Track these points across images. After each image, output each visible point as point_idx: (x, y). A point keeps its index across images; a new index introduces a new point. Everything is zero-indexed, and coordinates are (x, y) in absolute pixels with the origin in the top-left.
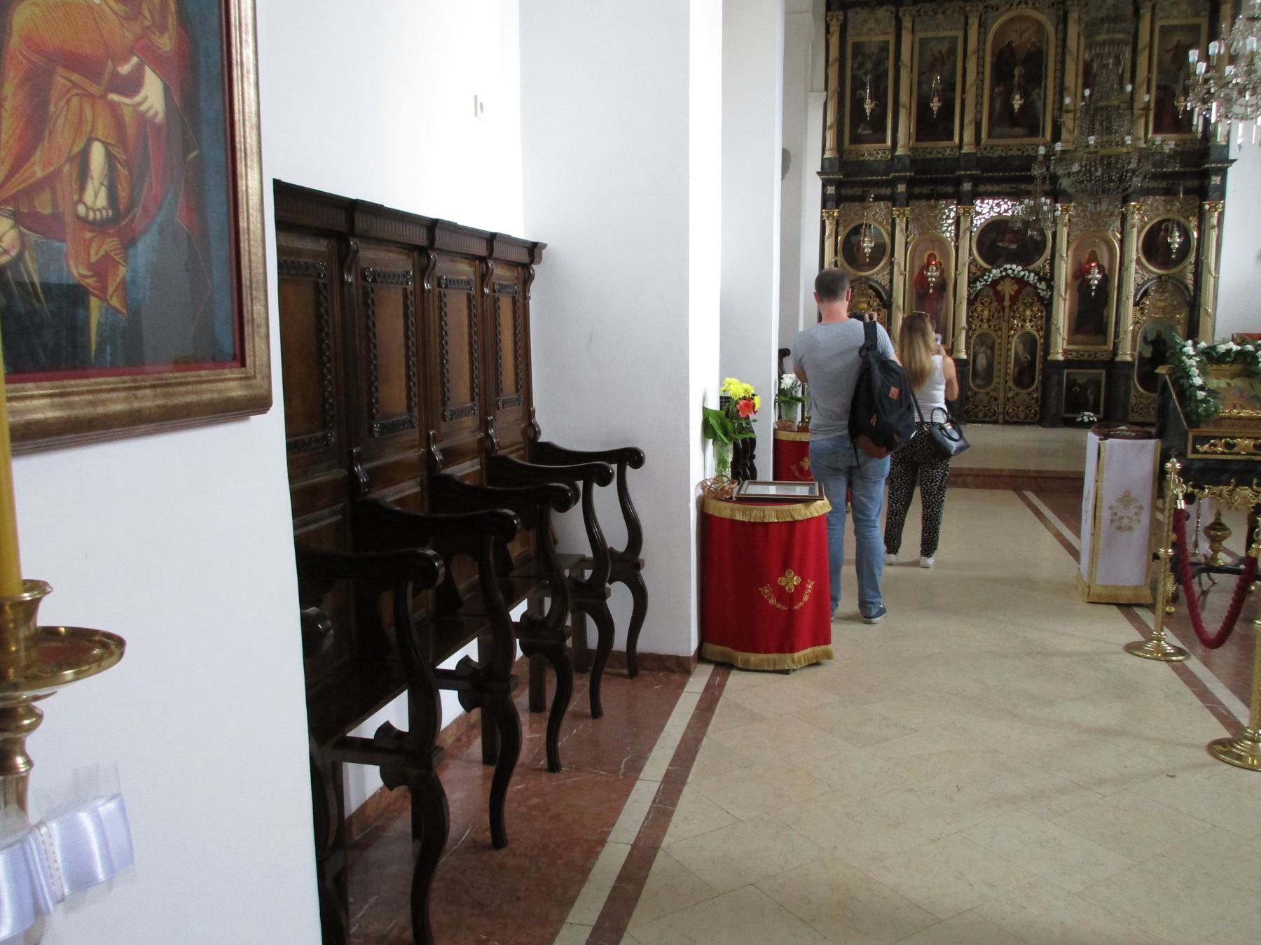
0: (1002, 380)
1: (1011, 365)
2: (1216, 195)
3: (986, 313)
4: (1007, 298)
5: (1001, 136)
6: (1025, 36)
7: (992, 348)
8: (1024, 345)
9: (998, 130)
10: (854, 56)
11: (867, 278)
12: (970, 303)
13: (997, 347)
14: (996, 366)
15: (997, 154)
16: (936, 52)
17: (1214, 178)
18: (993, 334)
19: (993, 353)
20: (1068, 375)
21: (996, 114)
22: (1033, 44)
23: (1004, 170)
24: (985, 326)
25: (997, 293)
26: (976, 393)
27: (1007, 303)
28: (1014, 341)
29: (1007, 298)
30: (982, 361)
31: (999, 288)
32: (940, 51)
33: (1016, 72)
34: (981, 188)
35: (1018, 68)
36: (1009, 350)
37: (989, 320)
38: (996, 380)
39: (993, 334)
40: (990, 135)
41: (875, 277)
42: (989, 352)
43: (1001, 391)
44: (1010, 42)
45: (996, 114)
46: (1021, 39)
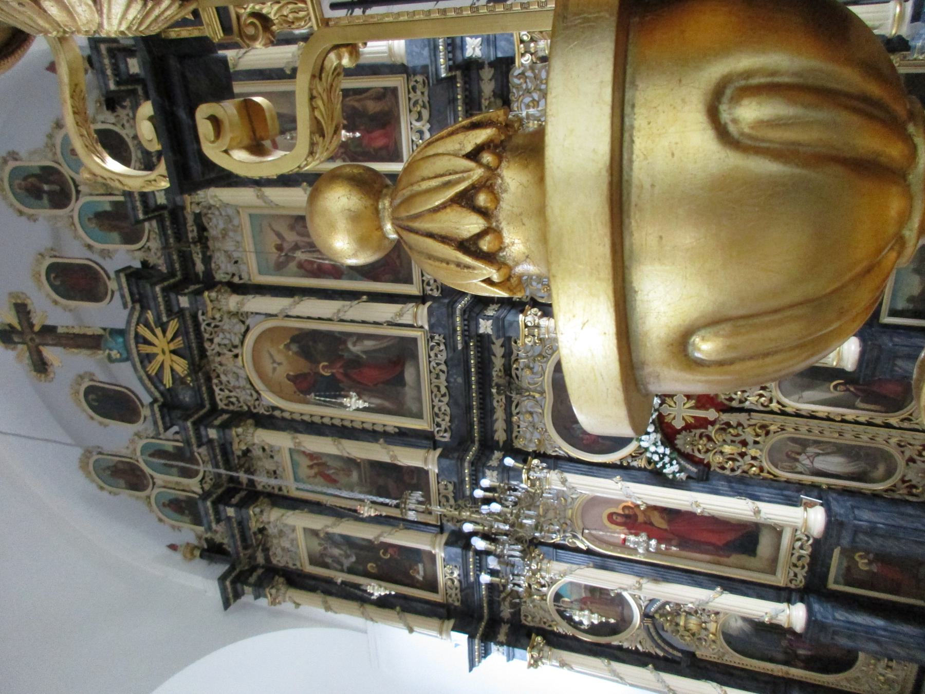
0: (884, 431)
1: (850, 414)
2: (502, 44)
3: (727, 449)
4: (701, 413)
5: (419, 400)
6: (279, 358)
7: (804, 444)
8: (808, 387)
9: (412, 405)
10: (326, 566)
11: (646, 615)
12: (703, 477)
13: (803, 434)
14: (848, 439)
15: (444, 407)
16: (313, 472)
17: (469, 53)
18: (773, 439)
19: (817, 443)
20: (893, 313)
21: (387, 404)
22: (287, 347)
23: (469, 408)
24: (753, 452)
25: (688, 427)
26: (904, 481)
27: (711, 414)
28: (792, 404)
29: (701, 413)
30: (834, 463)
31: (678, 424)
32: (311, 467)
33: (327, 373)
34: (500, 436)
35: (325, 362)
36: (812, 416)
37: (744, 443)
38: (880, 443)
39: (773, 439)
40: (419, 416)
41: (643, 605)
42: (811, 450)
43: (908, 435)
44: (289, 377)
45: (387, 404)
46: (283, 363)
